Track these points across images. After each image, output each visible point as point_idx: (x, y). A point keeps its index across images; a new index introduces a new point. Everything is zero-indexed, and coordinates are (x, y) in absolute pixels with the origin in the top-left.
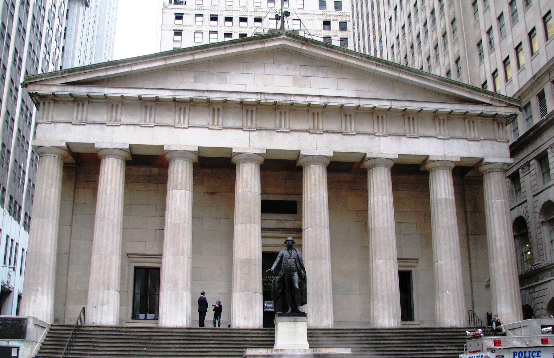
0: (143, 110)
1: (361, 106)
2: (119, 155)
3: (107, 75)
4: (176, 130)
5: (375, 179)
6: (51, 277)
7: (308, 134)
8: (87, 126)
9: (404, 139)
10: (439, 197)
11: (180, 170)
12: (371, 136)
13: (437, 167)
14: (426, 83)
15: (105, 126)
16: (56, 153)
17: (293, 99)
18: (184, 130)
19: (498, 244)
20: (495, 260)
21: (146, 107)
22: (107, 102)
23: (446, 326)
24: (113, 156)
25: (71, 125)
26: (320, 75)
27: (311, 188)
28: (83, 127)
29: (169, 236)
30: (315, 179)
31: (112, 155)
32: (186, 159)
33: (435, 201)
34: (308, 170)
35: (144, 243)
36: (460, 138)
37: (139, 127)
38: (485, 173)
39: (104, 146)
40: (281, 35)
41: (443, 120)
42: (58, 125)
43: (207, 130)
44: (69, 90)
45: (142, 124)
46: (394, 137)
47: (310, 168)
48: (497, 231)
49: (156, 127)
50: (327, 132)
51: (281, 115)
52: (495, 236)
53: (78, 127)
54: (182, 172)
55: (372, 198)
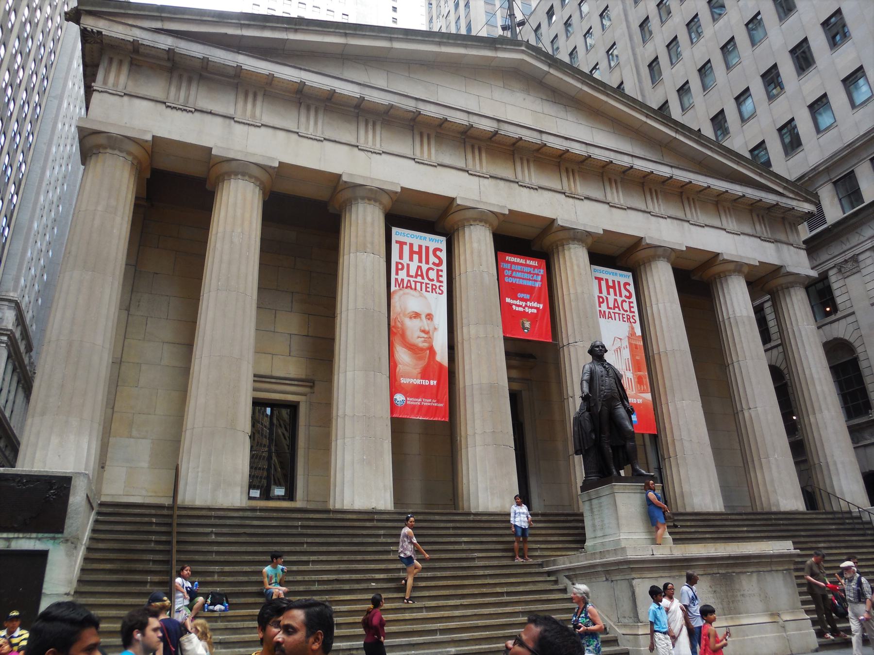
0: (303, 112)
1: (635, 167)
2: (257, 179)
3: (243, 37)
4: (362, 153)
5: (656, 277)
6: (100, 397)
7: (563, 196)
8: (197, 114)
9: (686, 224)
10: (738, 314)
11: (369, 219)
12: (646, 215)
13: (730, 271)
14: (709, 153)
15: (232, 122)
16: (129, 153)
17: (546, 138)
18: (374, 155)
19: (818, 388)
20: (817, 412)
21: (308, 109)
22: (237, 84)
23: (782, 509)
24: (247, 178)
25: (164, 107)
26: (570, 118)
27: (574, 280)
28: (190, 114)
29: (351, 333)
30: (579, 266)
31: (244, 174)
32: (377, 204)
33: (732, 320)
34: (566, 252)
35: (270, 356)
36: (752, 236)
37: (295, 136)
38: (779, 288)
39: (231, 155)
40: (521, 46)
41: (729, 208)
42: (137, 102)
43: (413, 162)
44: (165, 42)
45: (302, 131)
46: (675, 221)
47: (569, 249)
48: (814, 370)
49: (325, 143)
50: (588, 198)
51: (522, 163)
52: (813, 378)
53: (179, 112)
54: (373, 224)
55: (654, 307)
